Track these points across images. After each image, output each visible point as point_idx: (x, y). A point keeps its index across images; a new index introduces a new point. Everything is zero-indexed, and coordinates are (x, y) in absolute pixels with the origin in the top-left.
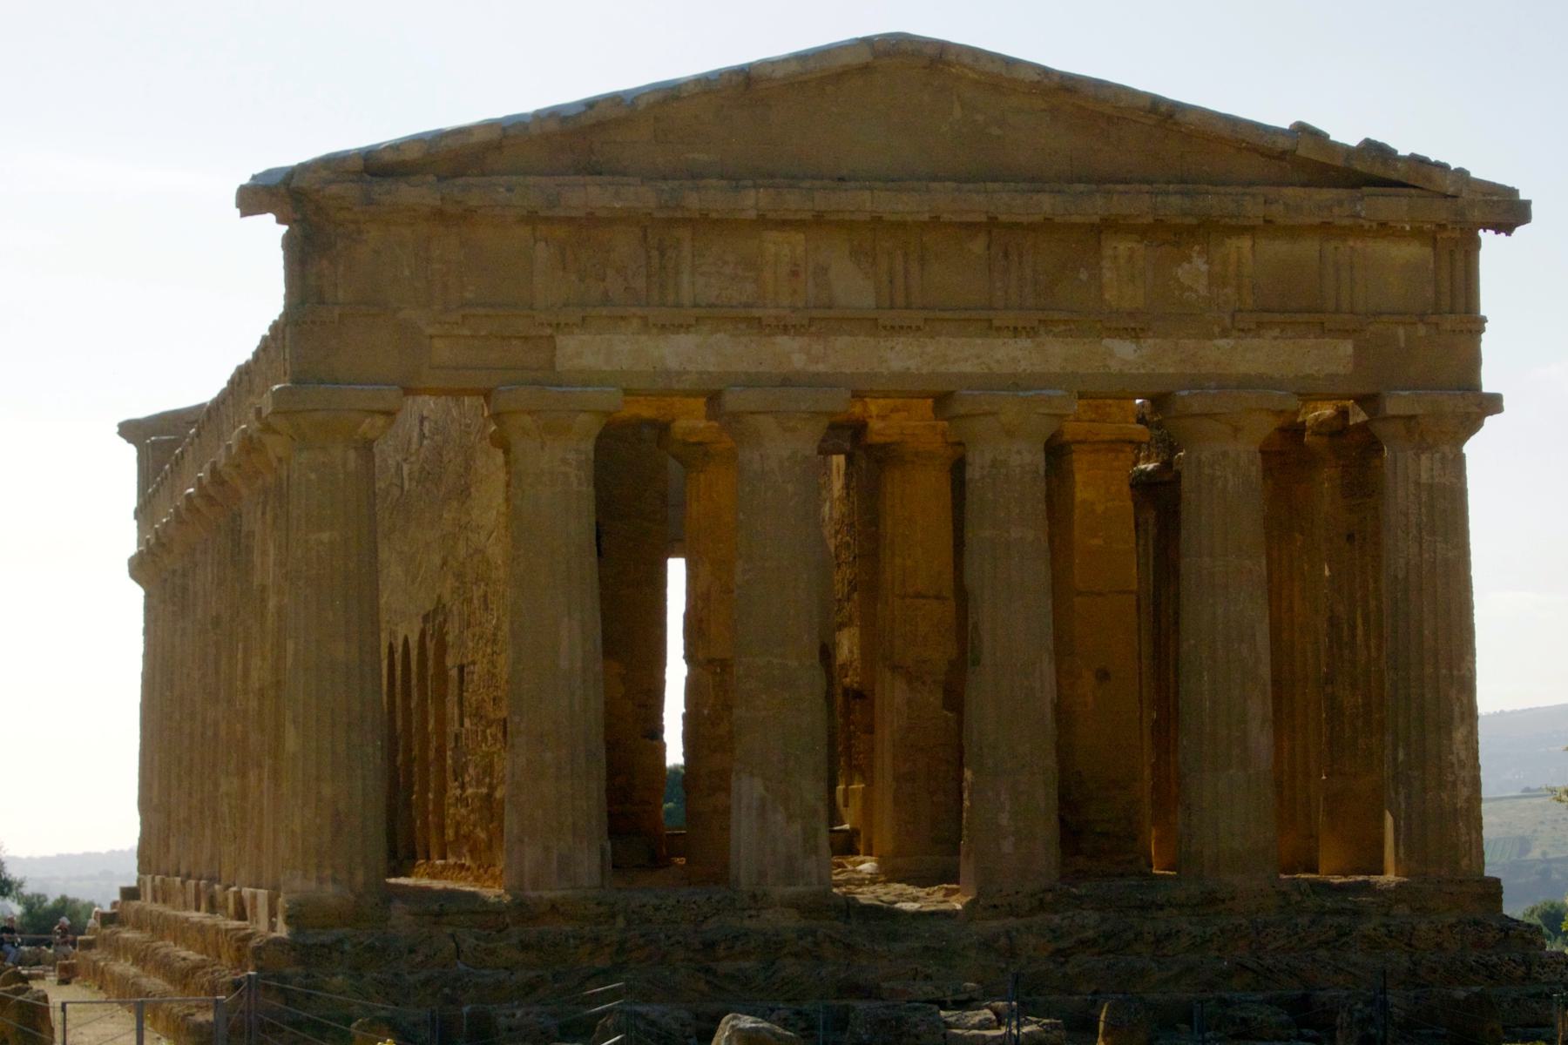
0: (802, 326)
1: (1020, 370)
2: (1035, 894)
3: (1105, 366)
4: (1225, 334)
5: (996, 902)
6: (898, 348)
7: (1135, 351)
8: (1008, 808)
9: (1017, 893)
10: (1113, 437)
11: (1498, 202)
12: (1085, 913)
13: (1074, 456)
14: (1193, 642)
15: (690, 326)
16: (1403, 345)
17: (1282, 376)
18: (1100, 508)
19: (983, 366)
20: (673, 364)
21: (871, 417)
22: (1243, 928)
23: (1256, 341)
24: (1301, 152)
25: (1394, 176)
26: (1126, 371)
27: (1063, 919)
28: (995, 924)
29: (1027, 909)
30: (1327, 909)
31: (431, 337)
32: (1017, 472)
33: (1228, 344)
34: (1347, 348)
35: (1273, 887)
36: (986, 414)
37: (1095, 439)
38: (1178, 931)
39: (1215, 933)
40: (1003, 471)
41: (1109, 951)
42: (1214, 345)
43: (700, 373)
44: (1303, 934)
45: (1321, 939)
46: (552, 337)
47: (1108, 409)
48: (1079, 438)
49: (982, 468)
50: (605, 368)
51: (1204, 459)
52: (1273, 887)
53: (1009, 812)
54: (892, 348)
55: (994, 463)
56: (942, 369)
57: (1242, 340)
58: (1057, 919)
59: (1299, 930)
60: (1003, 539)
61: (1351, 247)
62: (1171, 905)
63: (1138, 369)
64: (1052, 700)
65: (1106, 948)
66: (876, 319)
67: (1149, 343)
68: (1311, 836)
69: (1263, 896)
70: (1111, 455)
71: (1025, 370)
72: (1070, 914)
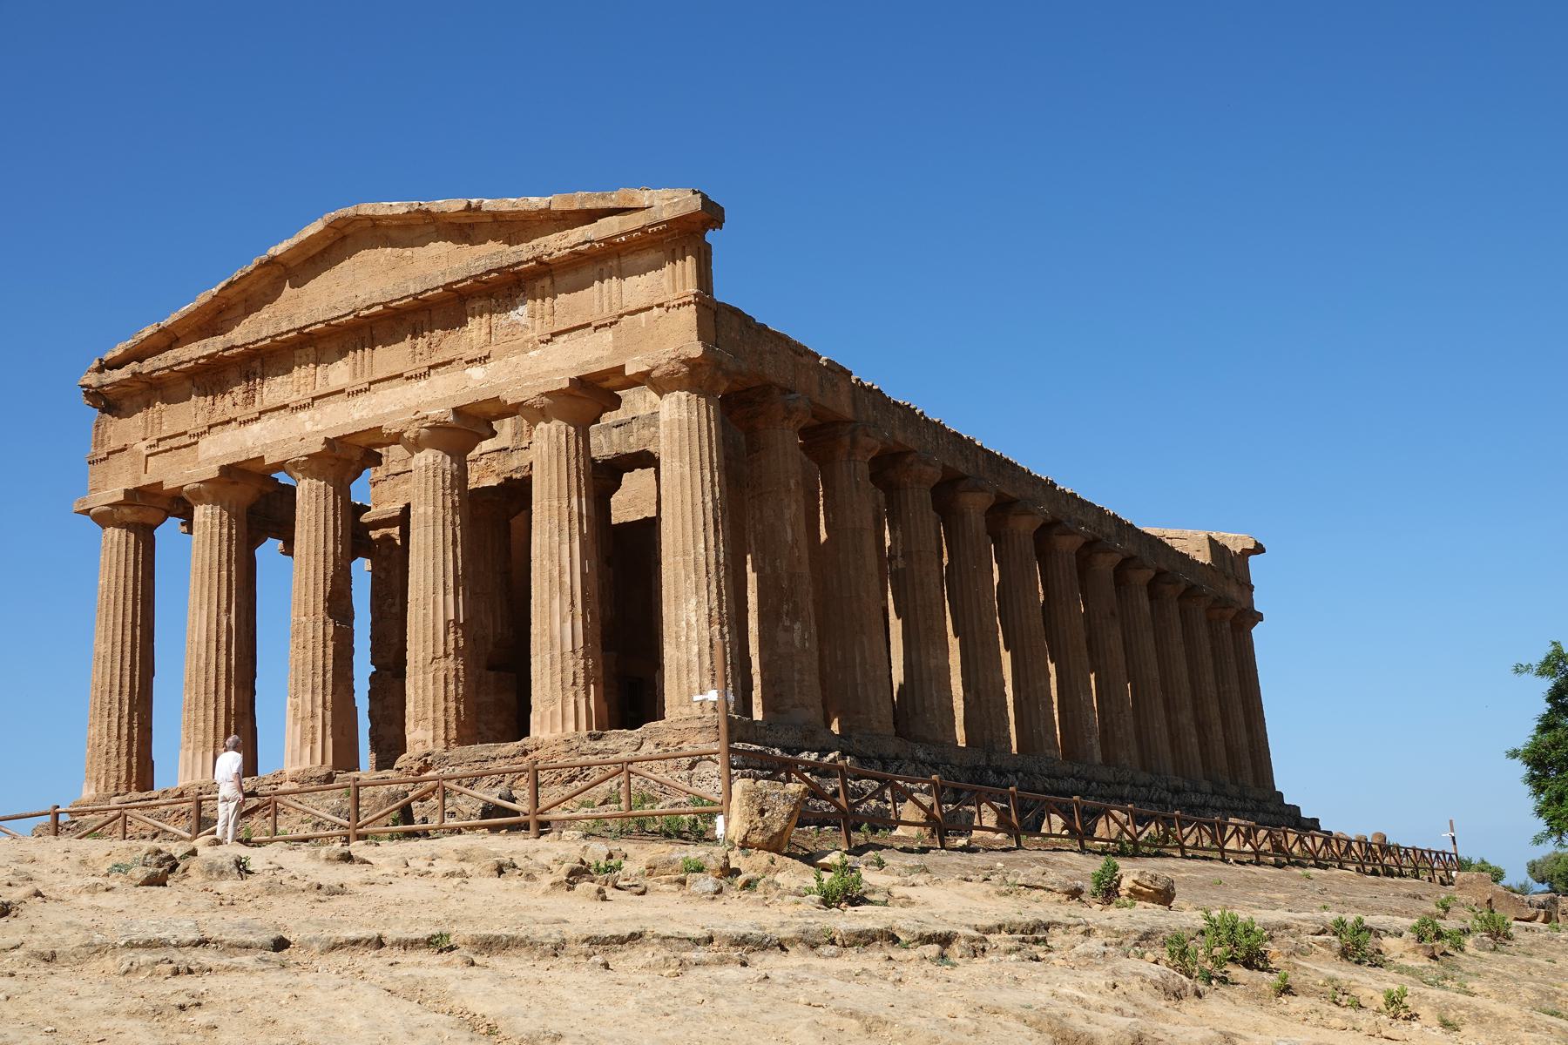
0: (309, 404)
4: (535, 348)
6: (358, 405)
11: (678, 202)
15: (257, 419)
16: (644, 325)
20: (250, 444)
24: (553, 208)
25: (612, 205)
31: (148, 456)
34: (607, 335)
43: (262, 445)
46: (196, 443)
50: (220, 454)
54: (355, 405)
56: (380, 412)
61: (611, 266)
66: (343, 391)
67: (491, 365)
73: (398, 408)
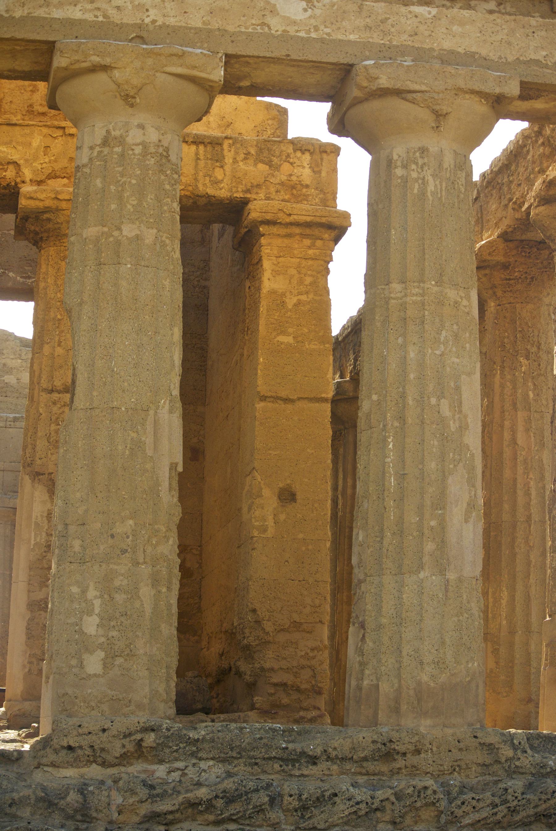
1: (147, 20)
2: (130, 734)
3: (263, 24)
5: (72, 744)
7: (305, 10)
8: (97, 610)
9: (104, 730)
10: (308, 219)
12: (203, 765)
13: (263, 241)
14: (375, 397)
17: (500, 58)
18: (291, 302)
19: (98, 13)
21: (23, 182)
22: (429, 792)
23: (466, 13)
26: (292, 33)
27: (169, 772)
28: (70, 774)
29: (118, 755)
30: (548, 770)
32: (137, 152)
33: (430, 13)
35: (475, 737)
36: (94, 69)
37: (288, 220)
38: (336, 795)
39: (387, 799)
40: (118, 149)
41: (230, 820)
42: (410, 12)
44: (516, 803)
45: (539, 809)
47: (304, 190)
48: (269, 217)
49: (91, 148)
51: (395, 157)
52: (475, 737)
53: (99, 615)
55: (105, 142)
57: (447, 9)
58: (161, 771)
59: (510, 797)
60: (111, 239)
62: (329, 759)
63: (309, 32)
64: (173, 466)
65: (226, 815)
68: (530, 700)
69: (460, 750)
70: (307, 242)
71: (154, 22)
72: (180, 764)
73: (89, 17)
